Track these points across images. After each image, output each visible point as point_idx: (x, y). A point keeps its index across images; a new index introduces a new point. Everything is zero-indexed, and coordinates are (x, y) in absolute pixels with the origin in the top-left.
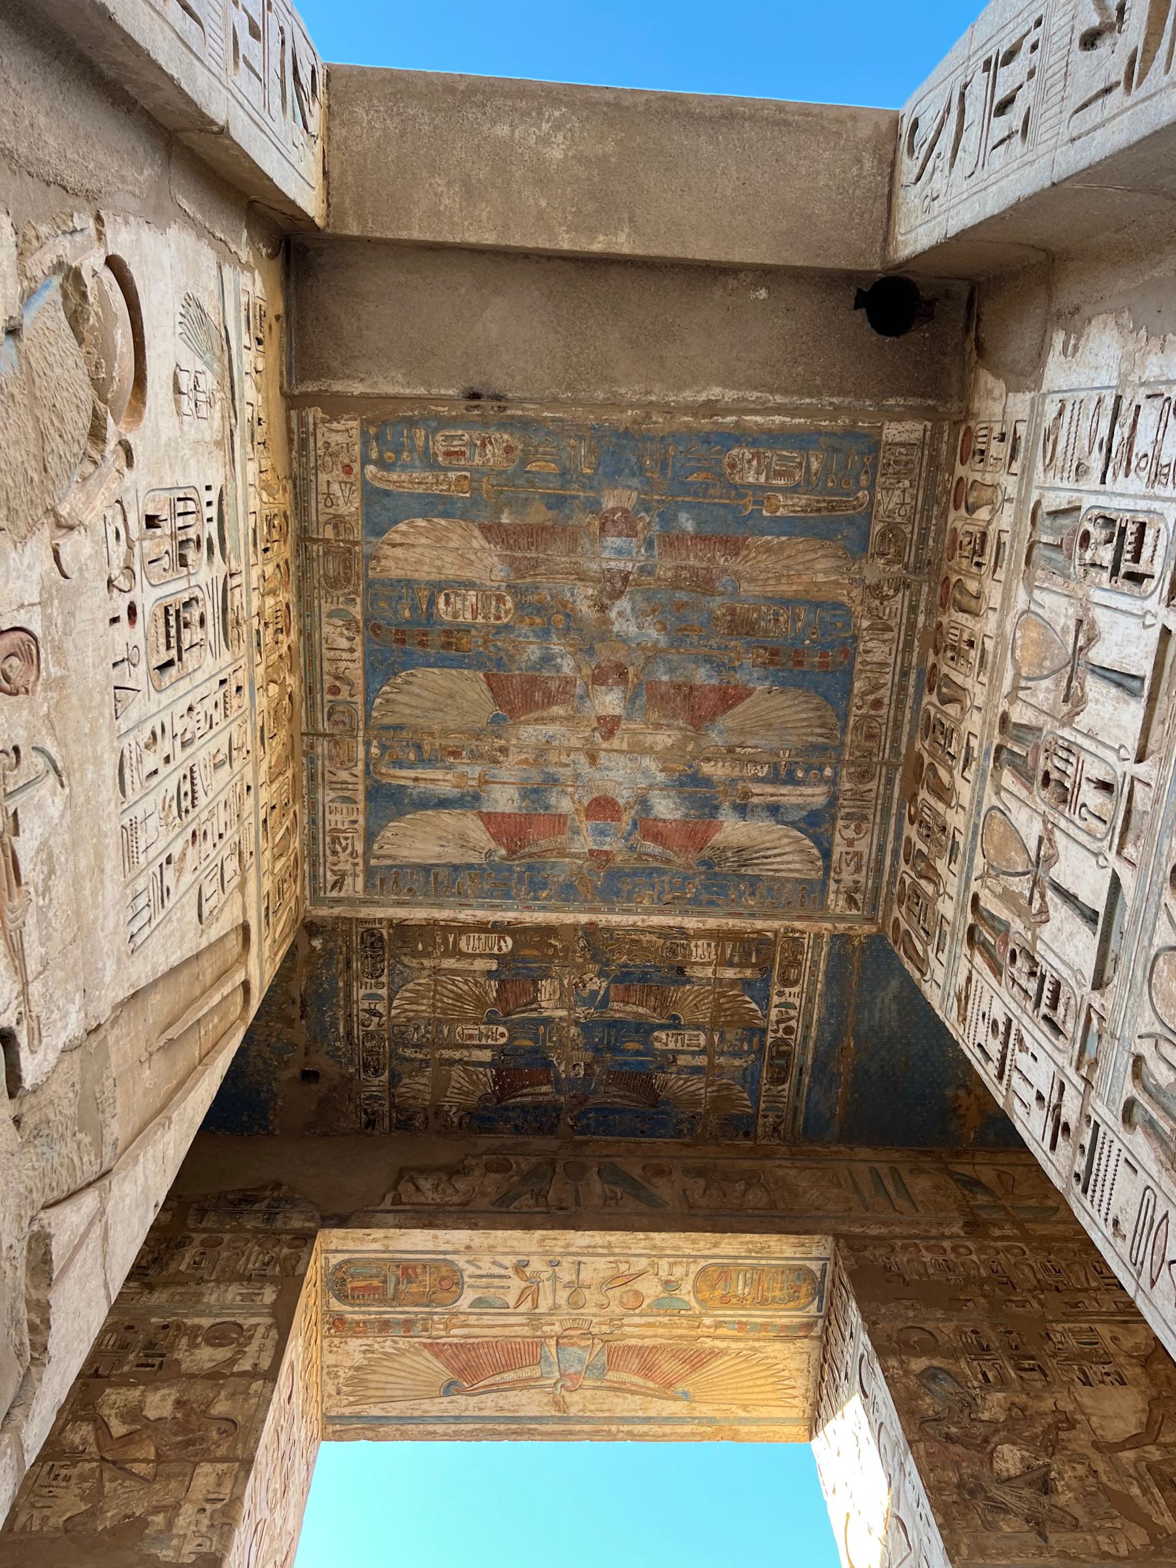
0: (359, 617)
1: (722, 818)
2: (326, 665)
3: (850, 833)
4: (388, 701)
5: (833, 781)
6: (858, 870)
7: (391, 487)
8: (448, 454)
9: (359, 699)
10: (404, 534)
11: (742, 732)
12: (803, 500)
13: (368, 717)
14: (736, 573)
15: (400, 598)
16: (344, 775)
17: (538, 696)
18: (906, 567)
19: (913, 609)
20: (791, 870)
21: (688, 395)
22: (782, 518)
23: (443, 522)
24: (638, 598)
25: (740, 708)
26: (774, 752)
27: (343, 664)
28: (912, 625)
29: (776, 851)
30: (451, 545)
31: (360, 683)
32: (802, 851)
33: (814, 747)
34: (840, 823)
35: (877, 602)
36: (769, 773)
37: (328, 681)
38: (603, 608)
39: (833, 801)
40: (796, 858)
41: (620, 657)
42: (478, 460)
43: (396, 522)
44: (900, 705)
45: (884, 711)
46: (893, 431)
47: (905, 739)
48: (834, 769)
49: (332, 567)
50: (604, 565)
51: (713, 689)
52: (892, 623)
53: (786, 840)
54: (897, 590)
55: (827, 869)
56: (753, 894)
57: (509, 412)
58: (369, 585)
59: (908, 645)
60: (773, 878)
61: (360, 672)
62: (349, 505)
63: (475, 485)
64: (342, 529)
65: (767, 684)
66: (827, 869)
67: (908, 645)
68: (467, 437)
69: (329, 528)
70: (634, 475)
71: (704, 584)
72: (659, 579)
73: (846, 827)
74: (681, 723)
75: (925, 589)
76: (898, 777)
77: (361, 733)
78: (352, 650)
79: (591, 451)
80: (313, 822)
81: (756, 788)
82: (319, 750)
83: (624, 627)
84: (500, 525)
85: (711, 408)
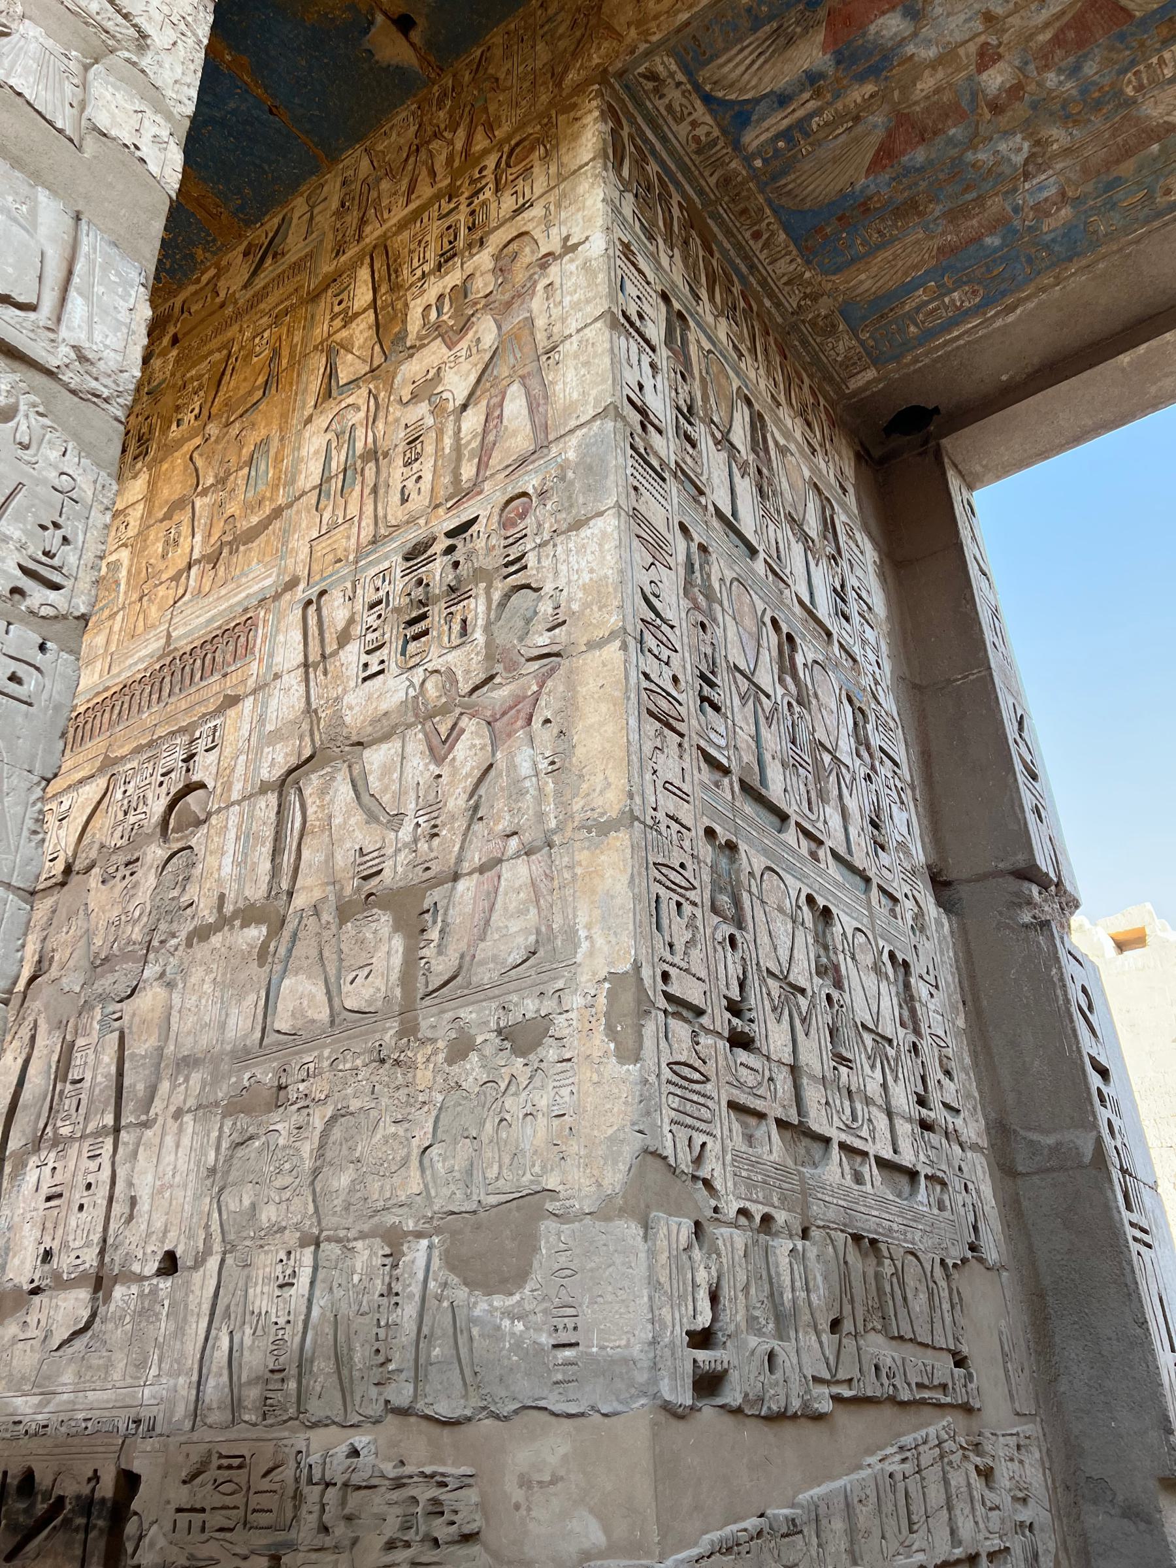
1: (828, 56)
3: (701, 132)
5: (748, 160)
6: (669, 108)
11: (857, 140)
12: (907, 308)
14: (932, 238)
17: (1071, 34)
18: (803, 322)
19: (778, 305)
20: (729, 61)
21: (1030, 305)
22: (917, 289)
24: (1008, 171)
25: (870, 156)
26: (818, 143)
28: (771, 295)
29: (756, 66)
32: (731, 85)
33: (784, 173)
34: (716, 132)
35: (808, 291)
36: (810, 125)
38: (1038, 143)
39: (737, 146)
40: (734, 76)
41: (1003, 120)
44: (739, 247)
45: (748, 235)
46: (871, 374)
47: (716, 229)
48: (755, 169)
50: (1051, 172)
51: (903, 153)
52: (787, 288)
53: (753, 83)
54: (799, 306)
55: (697, 88)
56: (749, 10)
59: (763, 283)
60: (741, 40)
65: (858, 187)
66: (697, 88)
67: (763, 283)
70: (1053, 240)
71: (954, 215)
72: (996, 194)
73: (708, 134)
74: (918, 109)
75: (780, 320)
76: (697, 200)
79: (1095, 232)
81: (812, 105)
83: (1011, 144)
84: (1159, 139)
85: (1011, 309)
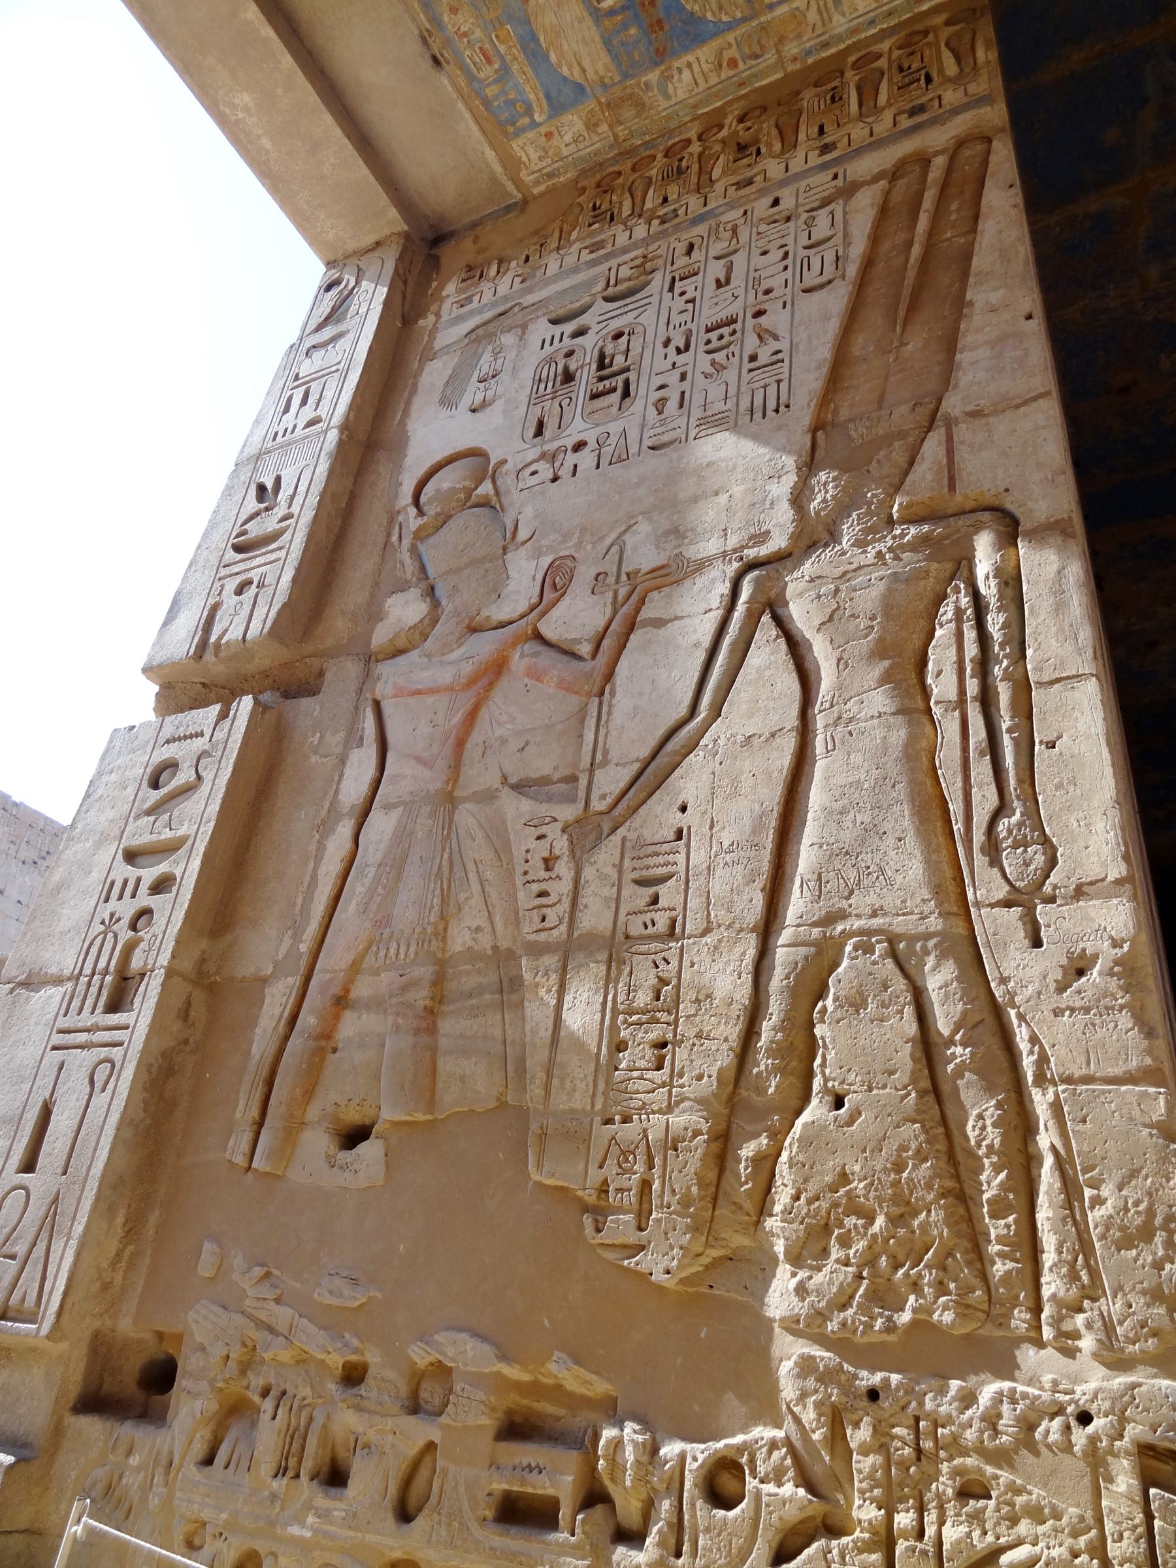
0: (657, 72)
2: (712, 82)
4: (721, 8)
7: (541, 95)
8: (489, 61)
9: (730, 37)
10: (570, 67)
13: (744, 20)
15: (623, 44)
16: (812, 16)
23: (542, 38)
27: (705, 67)
30: (555, 21)
31: (715, 44)
37: (726, 73)
42: (478, 33)
43: (565, 78)
49: (628, 113)
57: (428, 26)
58: (626, 76)
61: (705, 49)
62: (573, 123)
63: (497, 25)
64: (594, 120)
68: (468, 53)
69: (600, 130)
77: (763, 19)
78: (689, 65)
80: (872, 22)
82: (795, 51)
